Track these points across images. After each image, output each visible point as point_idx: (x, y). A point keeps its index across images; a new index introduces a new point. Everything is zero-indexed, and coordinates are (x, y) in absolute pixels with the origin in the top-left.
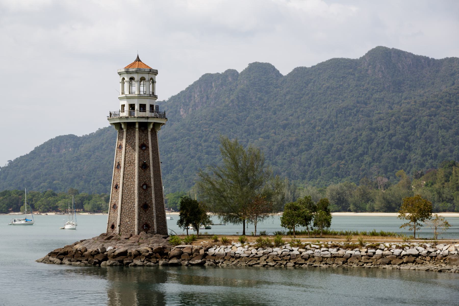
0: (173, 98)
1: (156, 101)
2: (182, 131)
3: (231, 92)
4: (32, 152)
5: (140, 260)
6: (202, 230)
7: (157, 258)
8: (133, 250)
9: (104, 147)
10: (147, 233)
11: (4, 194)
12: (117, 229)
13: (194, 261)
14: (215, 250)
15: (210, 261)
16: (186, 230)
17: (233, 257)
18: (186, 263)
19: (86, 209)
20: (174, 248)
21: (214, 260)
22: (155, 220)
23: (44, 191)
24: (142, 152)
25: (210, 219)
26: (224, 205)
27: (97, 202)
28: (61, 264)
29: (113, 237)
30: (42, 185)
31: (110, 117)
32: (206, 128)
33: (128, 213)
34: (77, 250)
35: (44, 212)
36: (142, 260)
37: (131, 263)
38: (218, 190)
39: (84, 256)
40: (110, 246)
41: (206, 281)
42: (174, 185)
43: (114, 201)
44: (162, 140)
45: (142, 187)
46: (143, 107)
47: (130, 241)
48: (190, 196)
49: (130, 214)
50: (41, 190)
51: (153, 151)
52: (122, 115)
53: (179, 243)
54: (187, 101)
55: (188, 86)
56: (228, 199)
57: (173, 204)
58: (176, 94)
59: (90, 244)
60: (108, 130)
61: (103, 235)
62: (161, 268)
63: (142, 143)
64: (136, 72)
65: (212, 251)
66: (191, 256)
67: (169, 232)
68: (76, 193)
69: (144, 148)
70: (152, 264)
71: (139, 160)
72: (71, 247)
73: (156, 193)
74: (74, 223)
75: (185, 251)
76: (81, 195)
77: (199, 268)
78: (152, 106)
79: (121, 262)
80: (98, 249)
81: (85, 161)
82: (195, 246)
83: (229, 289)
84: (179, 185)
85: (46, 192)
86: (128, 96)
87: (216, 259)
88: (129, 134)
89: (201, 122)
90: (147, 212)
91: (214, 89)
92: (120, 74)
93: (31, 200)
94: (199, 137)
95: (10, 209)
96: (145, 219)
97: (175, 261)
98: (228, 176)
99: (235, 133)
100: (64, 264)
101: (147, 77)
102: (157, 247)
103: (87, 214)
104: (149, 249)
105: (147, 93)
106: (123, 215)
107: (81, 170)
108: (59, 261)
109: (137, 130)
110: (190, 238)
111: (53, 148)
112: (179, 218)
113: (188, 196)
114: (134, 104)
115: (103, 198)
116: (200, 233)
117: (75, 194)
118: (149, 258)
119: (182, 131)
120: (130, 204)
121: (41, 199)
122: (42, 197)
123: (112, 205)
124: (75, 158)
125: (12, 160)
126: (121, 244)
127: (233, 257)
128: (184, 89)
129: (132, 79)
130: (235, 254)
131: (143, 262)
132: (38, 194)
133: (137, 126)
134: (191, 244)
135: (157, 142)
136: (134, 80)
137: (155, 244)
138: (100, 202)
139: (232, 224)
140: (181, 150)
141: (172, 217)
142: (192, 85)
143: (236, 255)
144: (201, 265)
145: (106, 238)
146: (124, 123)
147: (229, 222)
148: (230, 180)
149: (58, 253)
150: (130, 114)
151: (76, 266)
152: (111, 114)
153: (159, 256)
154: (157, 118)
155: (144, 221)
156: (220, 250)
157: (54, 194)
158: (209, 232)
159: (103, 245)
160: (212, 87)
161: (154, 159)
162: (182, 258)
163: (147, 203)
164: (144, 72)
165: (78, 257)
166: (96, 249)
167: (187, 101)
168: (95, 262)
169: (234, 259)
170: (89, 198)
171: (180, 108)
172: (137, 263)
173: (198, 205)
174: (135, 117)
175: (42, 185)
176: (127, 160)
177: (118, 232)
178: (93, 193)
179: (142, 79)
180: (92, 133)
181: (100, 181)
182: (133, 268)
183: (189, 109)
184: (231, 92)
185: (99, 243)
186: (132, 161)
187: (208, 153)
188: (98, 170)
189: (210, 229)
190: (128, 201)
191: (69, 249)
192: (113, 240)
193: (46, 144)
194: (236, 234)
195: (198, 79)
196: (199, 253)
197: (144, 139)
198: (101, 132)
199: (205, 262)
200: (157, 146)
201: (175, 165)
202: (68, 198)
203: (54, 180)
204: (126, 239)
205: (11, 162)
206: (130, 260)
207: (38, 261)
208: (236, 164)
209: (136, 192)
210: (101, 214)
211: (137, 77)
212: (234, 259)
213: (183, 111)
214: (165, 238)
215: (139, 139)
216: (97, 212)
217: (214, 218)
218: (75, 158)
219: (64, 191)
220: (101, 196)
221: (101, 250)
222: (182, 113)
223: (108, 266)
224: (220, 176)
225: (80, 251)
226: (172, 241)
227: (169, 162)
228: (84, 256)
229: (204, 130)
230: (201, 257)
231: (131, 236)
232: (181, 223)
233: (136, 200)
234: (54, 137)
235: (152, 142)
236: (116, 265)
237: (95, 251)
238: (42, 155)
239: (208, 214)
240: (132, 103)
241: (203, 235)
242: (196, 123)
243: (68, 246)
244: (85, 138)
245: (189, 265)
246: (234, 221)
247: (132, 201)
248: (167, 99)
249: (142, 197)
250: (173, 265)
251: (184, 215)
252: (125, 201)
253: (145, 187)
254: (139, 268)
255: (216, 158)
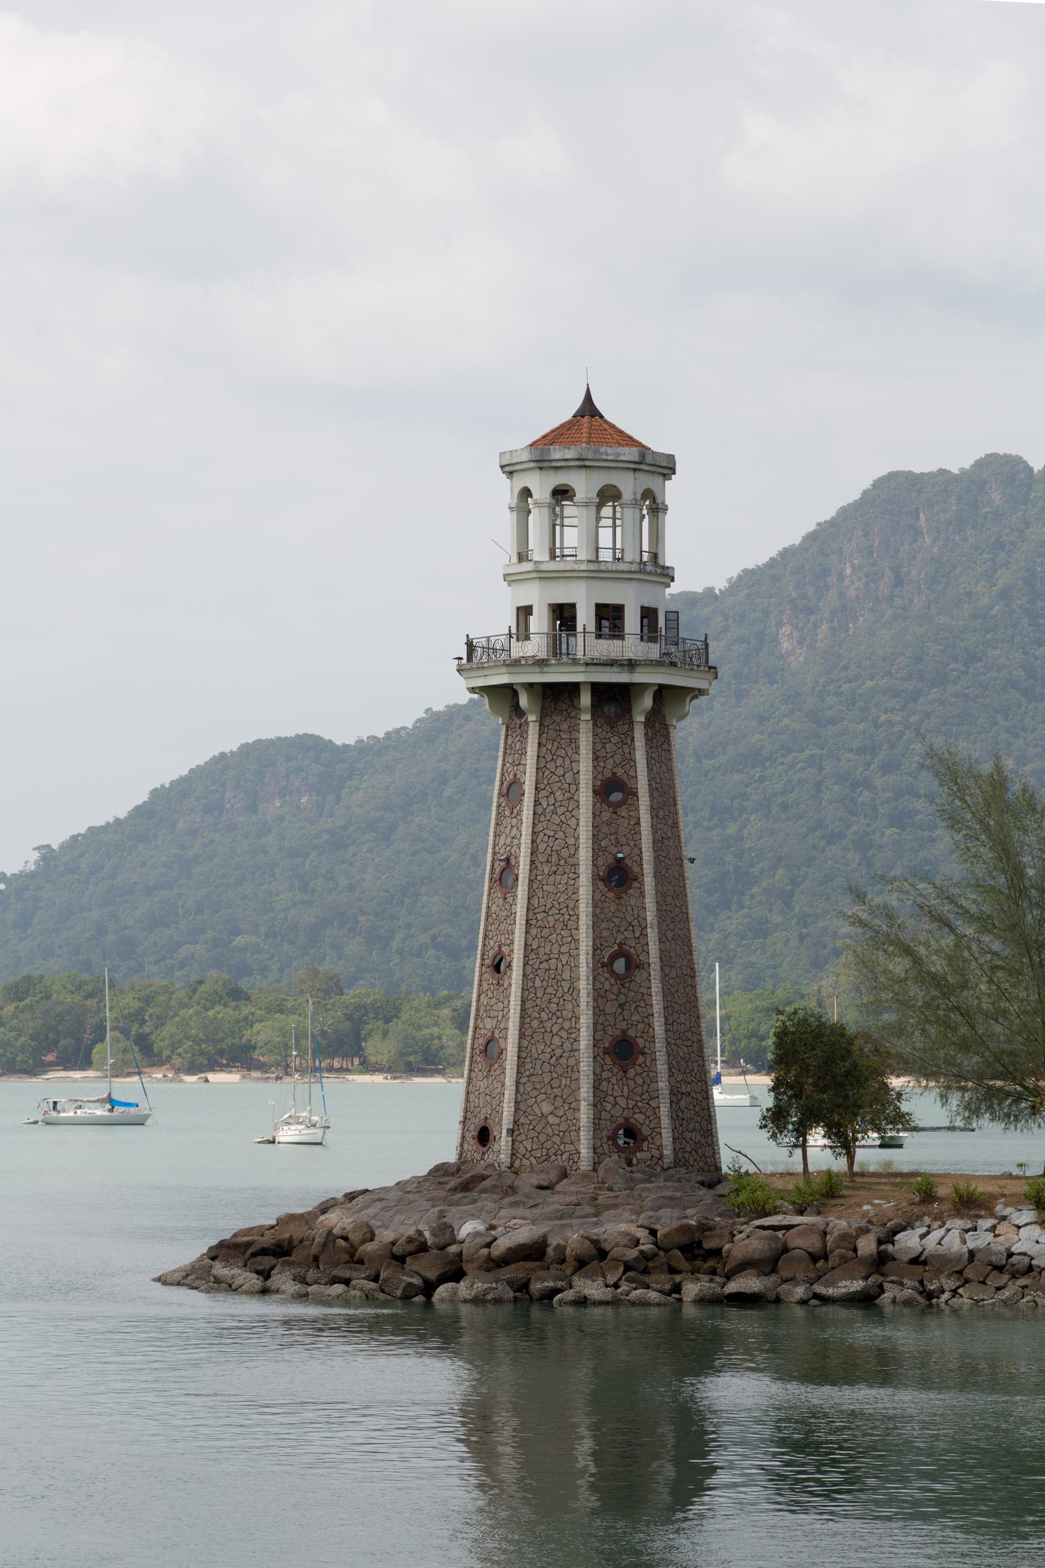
0: (750, 581)
1: (668, 591)
2: (785, 721)
3: (1002, 556)
4: (139, 812)
5: (600, 1281)
6: (869, 1154)
7: (673, 1271)
8: (572, 1238)
9: (449, 791)
10: (629, 1163)
11: (18, 991)
12: (503, 1144)
13: (833, 1284)
14: (923, 1237)
15: (901, 1284)
16: (799, 1152)
17: (999, 1268)
18: (800, 1291)
19: (372, 1059)
20: (747, 1229)
21: (921, 1282)
22: (664, 1110)
23: (194, 977)
24: (606, 815)
25: (905, 1107)
26: (964, 1046)
27: (420, 1028)
28: (264, 1291)
29: (484, 1178)
30: (184, 951)
31: (470, 658)
32: (893, 710)
33: (547, 1078)
34: (330, 1232)
35: (193, 1069)
36: (611, 1279)
37: (560, 1291)
38: (935, 980)
39: (361, 1262)
40: (474, 1216)
41: (883, 1368)
42: (753, 958)
43: (489, 1023)
44: (699, 760)
45: (609, 965)
46: (609, 617)
47: (556, 1198)
48: (820, 1004)
49: (555, 1083)
50: (178, 974)
51: (654, 810)
52: (519, 649)
53: (768, 1207)
54: (810, 591)
55: (812, 527)
56: (980, 1019)
57: (748, 1037)
58: (762, 560)
59: (386, 1208)
60: (468, 718)
61: (441, 1171)
62: (690, 1311)
63: (608, 774)
64: (583, 465)
65: (909, 1241)
66: (820, 1264)
67: (726, 1160)
68: (332, 987)
69: (616, 797)
70: (653, 1295)
71: (597, 851)
72: (306, 1219)
73: (667, 994)
74: (315, 1118)
75: (794, 1240)
76: (351, 996)
77: (856, 1313)
78: (648, 614)
79: (523, 1287)
80: (420, 1233)
81: (370, 851)
82: (839, 1223)
83: (978, 1400)
84: (772, 957)
85: (201, 982)
86: (543, 567)
87: (927, 1276)
88: (552, 733)
89: (869, 684)
90: (631, 1072)
91: (928, 541)
92: (509, 470)
93: (137, 1017)
94: (861, 751)
95: (50, 1058)
96: (622, 1102)
97: (748, 1283)
98: (983, 922)
99: (1016, 736)
100: (278, 1291)
101: (628, 485)
102: (676, 1224)
103: (378, 1078)
104: (642, 1234)
105: (628, 557)
106: (529, 1087)
107: (351, 888)
108: (254, 1281)
109: (586, 717)
110: (817, 1184)
111: (229, 795)
112: (768, 1101)
113: (813, 1004)
114: (573, 606)
115: (446, 1012)
116: (862, 1165)
117: (327, 993)
118: (639, 1269)
119: (785, 721)
120: (556, 1041)
121: (182, 1012)
122: (182, 1005)
123: (482, 1041)
124: (326, 837)
125: (55, 847)
126: (520, 1211)
127: (999, 1268)
128: (797, 540)
129: (562, 493)
130: (1010, 1255)
131: (616, 1286)
132: (168, 991)
133: (586, 699)
134: (819, 1213)
135: (670, 770)
136: (571, 498)
137: (666, 1213)
138: (435, 1030)
139: (998, 1127)
140: (785, 807)
141: (739, 1098)
142: (832, 523)
143: (1015, 1259)
144: (866, 1301)
145: (453, 1182)
146: (531, 685)
147: (985, 1121)
148: (986, 938)
149: (248, 1244)
150: (555, 648)
151: (327, 1303)
152: (470, 646)
153: (683, 1264)
154: (673, 664)
155: (617, 1112)
156: (948, 1238)
157: (237, 995)
158: (902, 1159)
159: (442, 1215)
160: (918, 533)
161: (658, 843)
162: (785, 1273)
163: (632, 1033)
164: (617, 466)
165: (336, 1265)
166: (411, 1232)
167: (810, 591)
168: (410, 1285)
169: (1006, 1277)
170: (387, 1012)
171: (780, 624)
172: (587, 1292)
173: (850, 1043)
174: (575, 662)
175: (184, 951)
176: (542, 847)
177: (504, 1157)
178: (403, 987)
179: (608, 495)
180: (397, 731)
181: (434, 938)
182: (570, 1311)
183: (816, 626)
184: (1002, 556)
185: (427, 1205)
186: (565, 853)
187: (898, 820)
188: (422, 890)
189: (900, 1146)
190: (548, 1025)
191: (296, 1232)
192: (484, 1191)
193: (197, 774)
194: (1016, 1172)
195: (857, 496)
196: (855, 1250)
197: (618, 758)
198: (437, 726)
199: (883, 1291)
200: (672, 786)
201: (755, 870)
202: (293, 1011)
203: (238, 933)
204: (541, 1188)
205: (47, 854)
206: (557, 1278)
207: (163, 1280)
208: (1017, 872)
209: (584, 986)
210: (438, 1080)
211: (584, 485)
212: (1006, 1277)
213: (790, 636)
214: (711, 1186)
215: (596, 758)
216: (422, 1072)
217: (921, 1100)
218: (326, 837)
219: (278, 981)
220: (438, 1005)
221: (434, 1234)
222: (785, 645)
223: (465, 1301)
224: (944, 922)
225: (345, 1238)
226: (739, 1200)
227: (729, 858)
228: (361, 1262)
229: (883, 718)
230: (864, 1272)
231: (564, 1175)
232: (776, 1119)
233: (585, 1020)
234: (232, 745)
235: (650, 769)
236: (497, 1301)
237: (410, 1240)
238: (181, 825)
239: (896, 1082)
240: (562, 597)
241: (873, 1175)
242: (846, 686)
243: (291, 1218)
244: (370, 752)
245: (814, 1302)
246: (1008, 1115)
247: (567, 1025)
248: (720, 584)
249: (611, 1008)
250: (742, 1300)
251: (789, 1086)
252: (535, 1024)
253: (620, 965)
254: (597, 1312)
255: (932, 840)
